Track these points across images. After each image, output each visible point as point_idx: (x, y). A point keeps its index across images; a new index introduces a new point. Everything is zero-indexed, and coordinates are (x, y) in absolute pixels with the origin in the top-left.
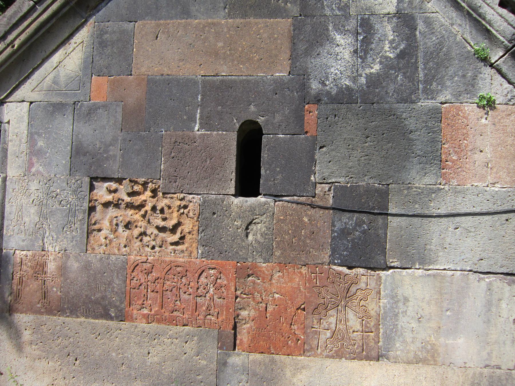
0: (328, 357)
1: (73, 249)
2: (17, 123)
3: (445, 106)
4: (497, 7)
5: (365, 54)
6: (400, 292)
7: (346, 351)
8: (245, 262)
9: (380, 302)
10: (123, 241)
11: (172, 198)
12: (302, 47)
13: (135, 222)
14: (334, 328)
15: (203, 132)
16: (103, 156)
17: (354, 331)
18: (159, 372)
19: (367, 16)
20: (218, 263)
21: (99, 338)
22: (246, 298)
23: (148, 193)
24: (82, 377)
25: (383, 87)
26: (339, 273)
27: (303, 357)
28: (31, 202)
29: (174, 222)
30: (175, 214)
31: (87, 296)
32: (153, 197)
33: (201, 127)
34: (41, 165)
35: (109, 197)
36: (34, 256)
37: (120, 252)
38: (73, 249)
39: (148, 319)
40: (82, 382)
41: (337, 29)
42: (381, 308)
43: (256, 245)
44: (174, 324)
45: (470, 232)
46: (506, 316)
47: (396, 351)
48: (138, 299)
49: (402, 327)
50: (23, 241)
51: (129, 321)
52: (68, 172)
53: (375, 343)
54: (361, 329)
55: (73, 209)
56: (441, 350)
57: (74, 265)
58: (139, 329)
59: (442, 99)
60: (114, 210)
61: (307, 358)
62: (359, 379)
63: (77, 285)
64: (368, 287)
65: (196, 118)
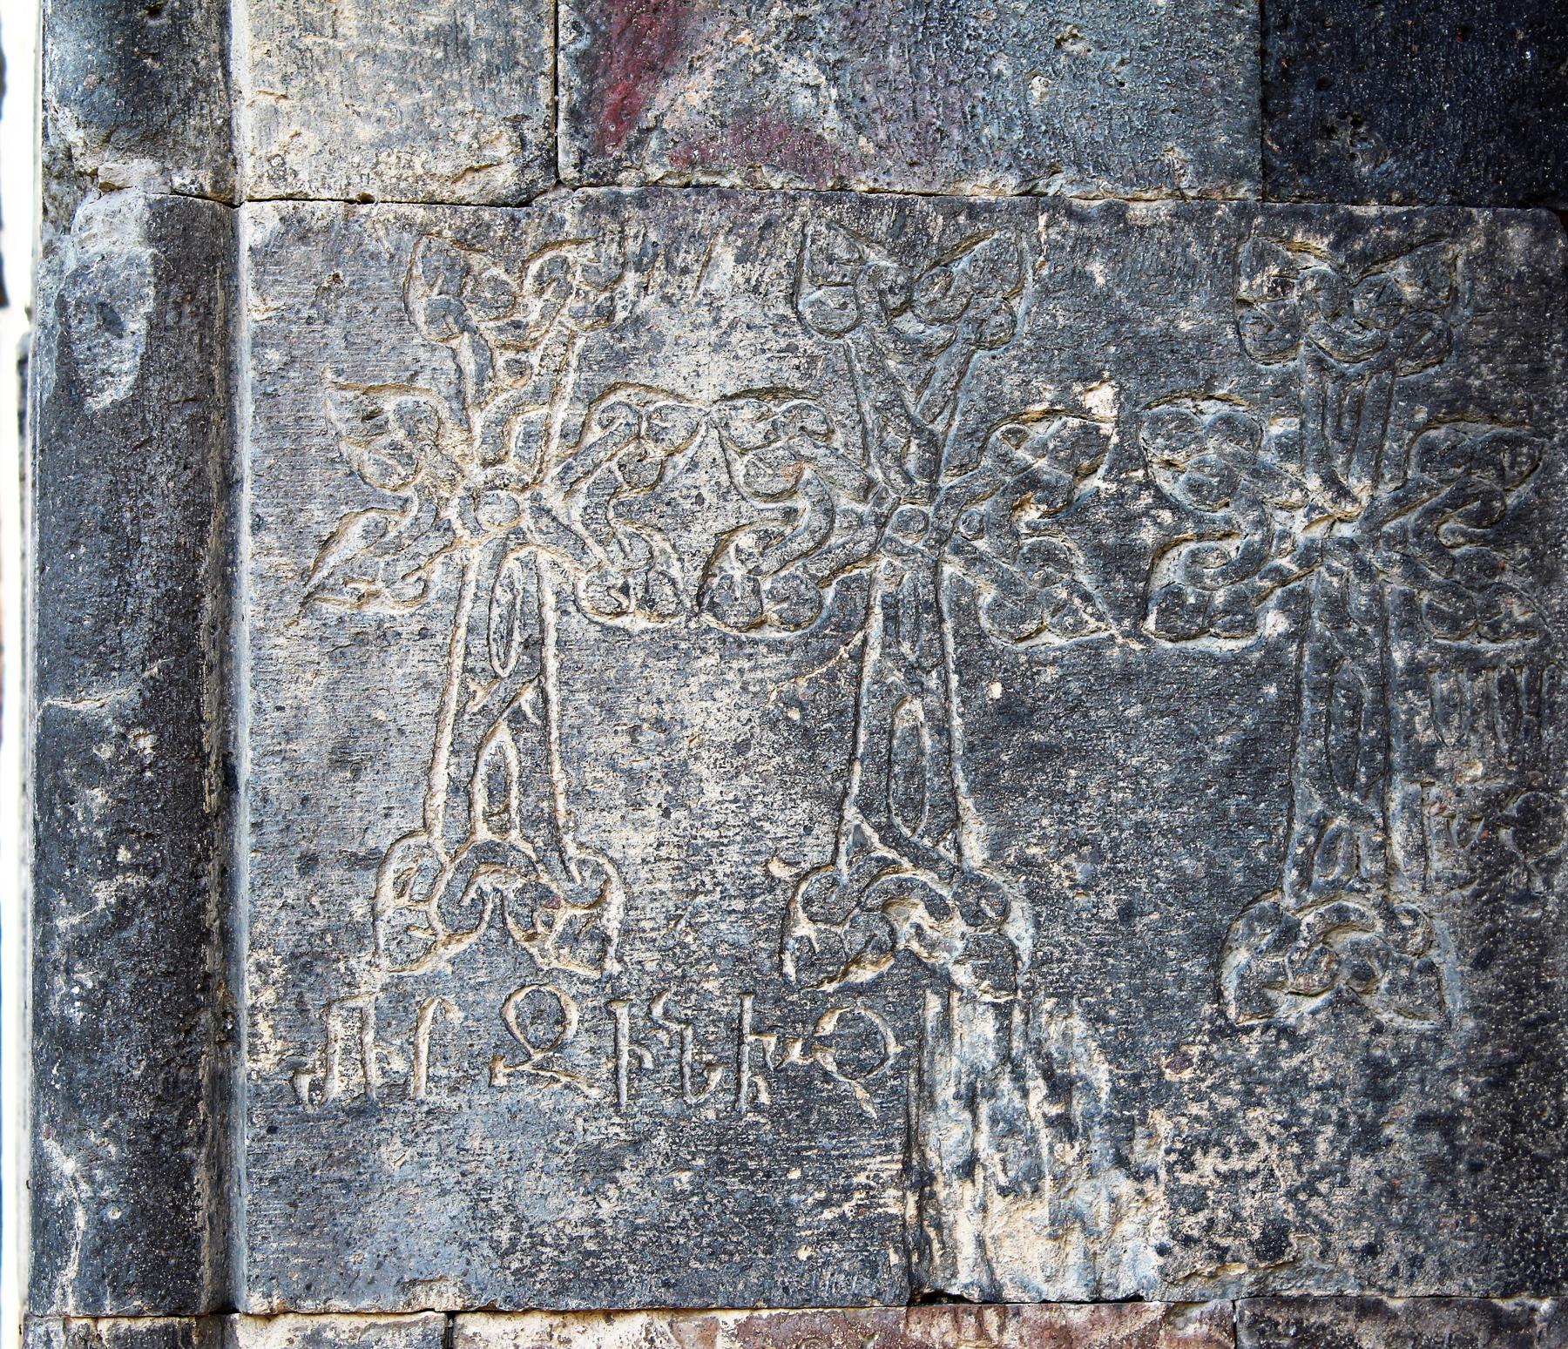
1: (1395, 1250)
28: (686, 575)
34: (798, 36)
38: (1395, 1250)
50: (598, 1167)
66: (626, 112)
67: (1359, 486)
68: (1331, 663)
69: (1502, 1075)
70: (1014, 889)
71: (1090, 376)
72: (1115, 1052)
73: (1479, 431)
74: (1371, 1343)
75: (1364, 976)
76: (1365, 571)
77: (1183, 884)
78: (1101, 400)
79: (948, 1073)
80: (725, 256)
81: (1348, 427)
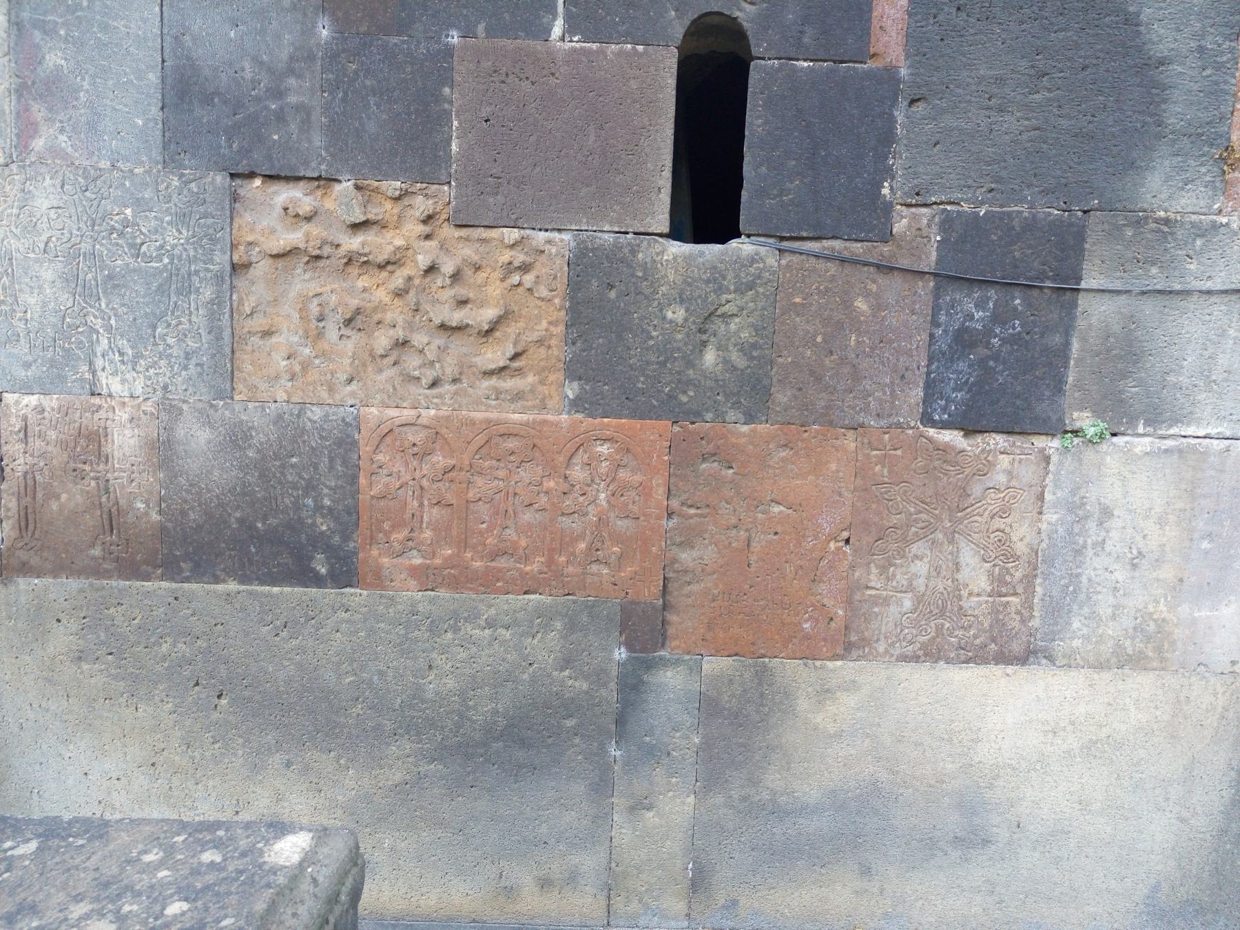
0: (904, 658)
1: (191, 390)
6: (1092, 494)
7: (949, 643)
8: (693, 423)
9: (1040, 520)
10: (344, 367)
13: (375, 309)
14: (922, 589)
15: (576, 43)
16: (266, 108)
17: (970, 594)
21: (284, 634)
22: (696, 515)
24: (241, 741)
26: (944, 449)
27: (839, 663)
28: (42, 246)
30: (495, 290)
31: (241, 521)
32: (428, 237)
33: (570, 29)
34: (62, 130)
36: (65, 411)
37: (337, 397)
38: (191, 390)
39: (427, 578)
40: (240, 752)
42: (1044, 535)
47: (1072, 638)
48: (393, 527)
49: (1090, 580)
50: (27, 365)
52: (156, 154)
53: (1023, 621)
54: (989, 589)
55: (183, 271)
56: (1179, 633)
57: (197, 437)
60: (307, 276)
61: (851, 664)
62: (978, 710)
63: (209, 491)
64: (1013, 483)
66: (26, 147)
67: (184, 231)
68: (178, 270)
70: (111, 313)
71: (126, 206)
72: (132, 348)
74: (185, 407)
75: (186, 336)
76: (185, 250)
77: (146, 314)
78: (128, 211)
79: (99, 350)
80: (48, 178)
81: (182, 218)
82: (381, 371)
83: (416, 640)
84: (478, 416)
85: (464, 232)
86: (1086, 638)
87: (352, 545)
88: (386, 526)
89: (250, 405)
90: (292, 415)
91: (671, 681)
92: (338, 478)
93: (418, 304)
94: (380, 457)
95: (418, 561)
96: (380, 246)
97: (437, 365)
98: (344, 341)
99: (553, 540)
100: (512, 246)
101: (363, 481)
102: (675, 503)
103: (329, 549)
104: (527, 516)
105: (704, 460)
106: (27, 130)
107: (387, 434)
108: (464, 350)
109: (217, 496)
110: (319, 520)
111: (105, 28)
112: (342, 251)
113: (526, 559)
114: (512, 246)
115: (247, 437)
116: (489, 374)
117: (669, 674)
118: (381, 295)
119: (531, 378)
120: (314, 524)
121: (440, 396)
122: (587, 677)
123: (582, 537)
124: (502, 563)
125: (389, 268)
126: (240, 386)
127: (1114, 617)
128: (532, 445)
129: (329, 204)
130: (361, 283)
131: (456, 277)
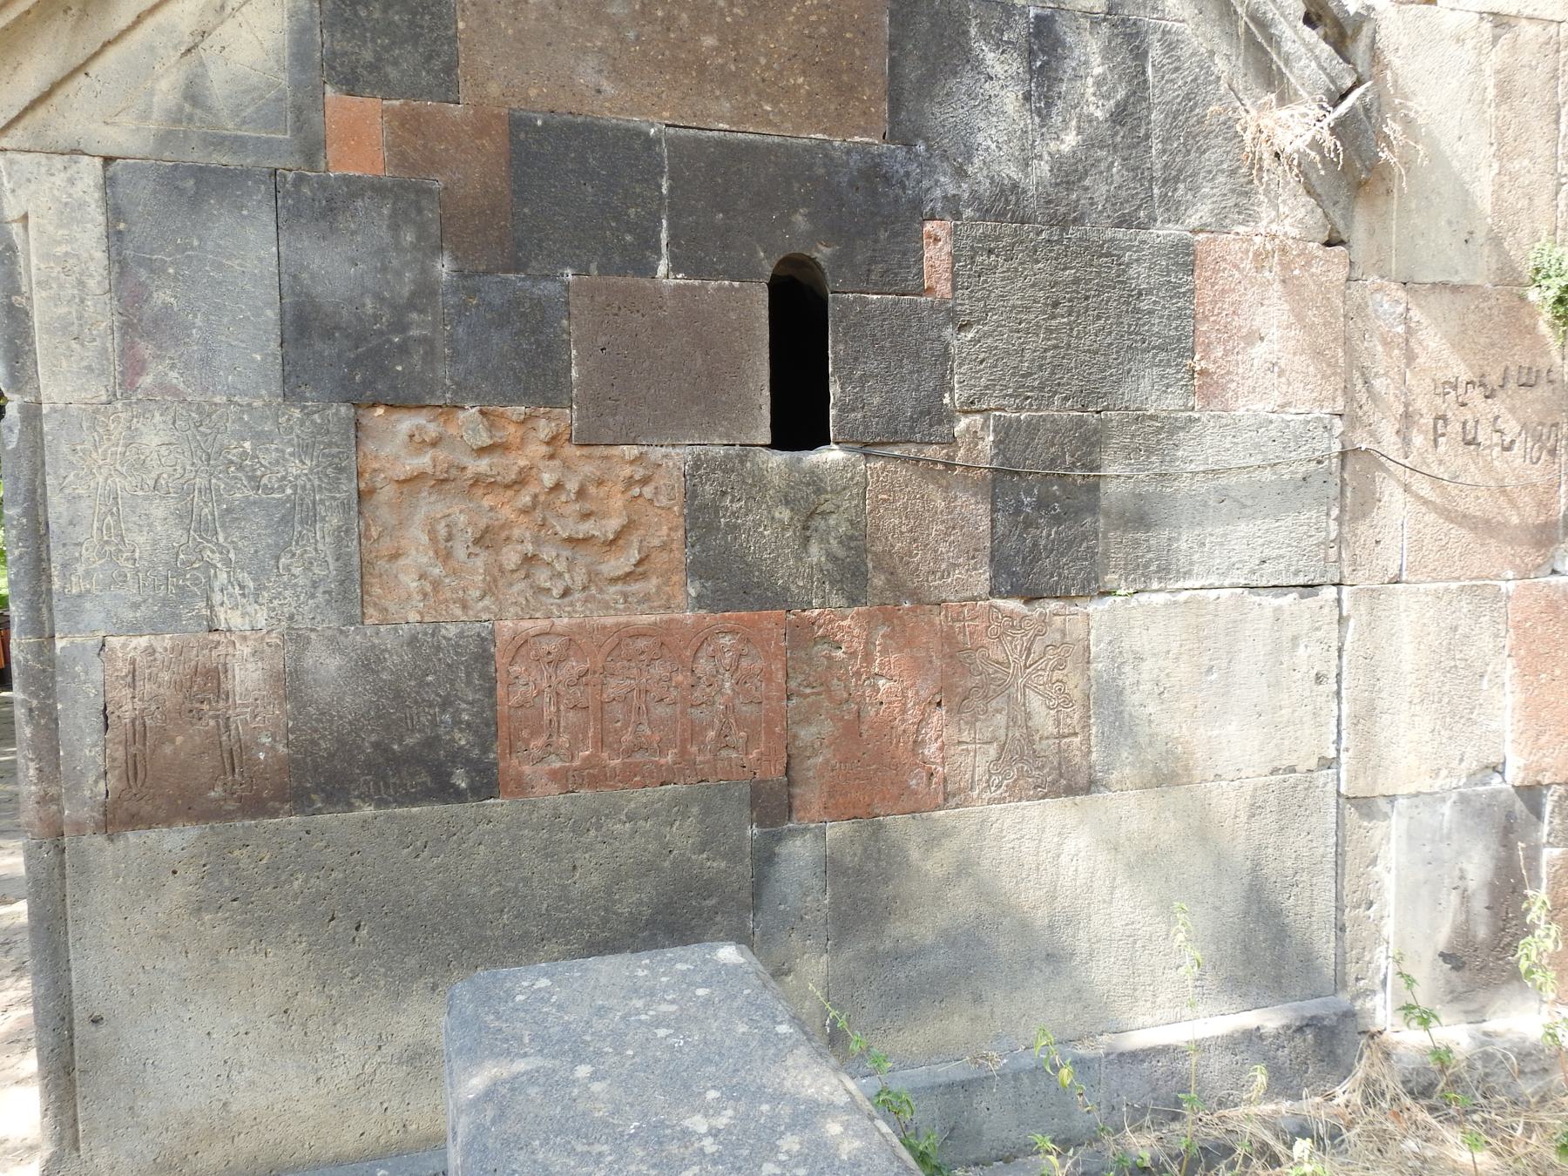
2: (59, 226)
3: (1201, 237)
4: (1300, 24)
5: (1049, 105)
11: (607, 458)
12: (912, 72)
13: (502, 527)
15: (680, 279)
16: (390, 341)
18: (606, 910)
19: (1048, 12)
20: (741, 618)
23: (537, 450)
25: (1086, 189)
28: (151, 483)
29: (613, 524)
30: (618, 502)
31: (376, 745)
32: (552, 457)
33: (676, 268)
34: (173, 367)
35: (424, 461)
36: (179, 651)
38: (319, 618)
39: (567, 780)
40: (382, 983)
41: (987, 37)
43: (830, 566)
44: (636, 786)
45: (1244, 506)
46: (1304, 669)
48: (532, 734)
51: (512, 794)
52: (276, 387)
55: (307, 501)
57: (326, 664)
58: (543, 812)
59: (1193, 221)
60: (433, 499)
63: (341, 718)
65: (659, 241)
66: (132, 384)
67: (308, 462)
69: (342, 583)
70: (230, 547)
71: (244, 440)
72: (254, 580)
73: (335, 450)
74: (313, 636)
77: (268, 546)
78: (247, 445)
79: (217, 585)
80: (157, 414)
81: (305, 449)
82: (511, 584)
83: (560, 842)
84: (610, 621)
85: (586, 451)
86: (1132, 764)
87: (492, 756)
88: (525, 734)
89: (382, 628)
90: (426, 634)
91: (799, 852)
92: (475, 692)
93: (544, 519)
94: (516, 668)
95: (558, 765)
96: (507, 467)
97: (567, 576)
98: (473, 558)
99: (684, 730)
100: (632, 462)
101: (501, 691)
102: (793, 684)
103: (470, 764)
104: (660, 711)
105: (816, 643)
106: (133, 367)
107: (521, 644)
108: (589, 559)
109: (350, 723)
110: (457, 735)
111: (220, 267)
112: (469, 473)
113: (662, 753)
114: (632, 462)
115: (379, 661)
116: (614, 580)
117: (798, 843)
118: (507, 513)
119: (654, 581)
120: (453, 740)
121: (572, 604)
122: (724, 857)
123: (711, 725)
124: (638, 757)
125: (516, 487)
126: (370, 611)
127: (1150, 744)
128: (663, 640)
129: (452, 430)
130: (487, 502)
131: (581, 493)
